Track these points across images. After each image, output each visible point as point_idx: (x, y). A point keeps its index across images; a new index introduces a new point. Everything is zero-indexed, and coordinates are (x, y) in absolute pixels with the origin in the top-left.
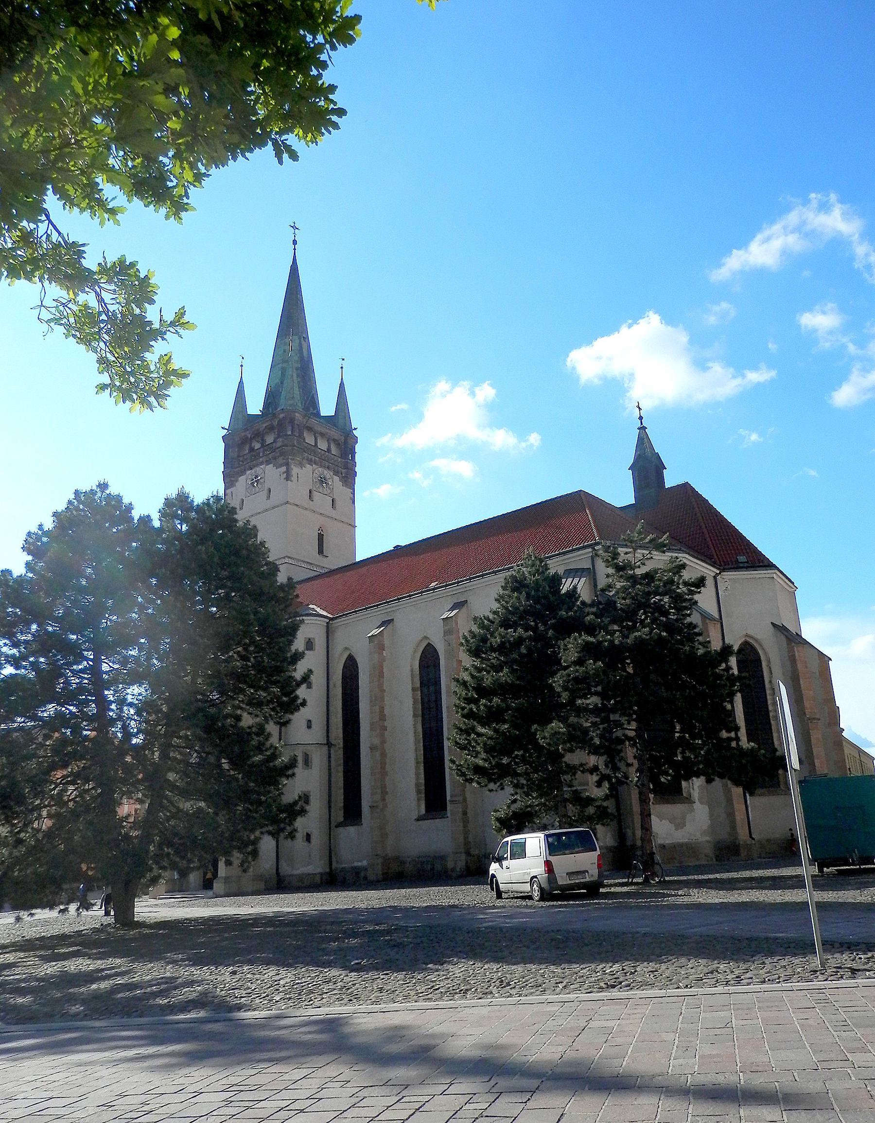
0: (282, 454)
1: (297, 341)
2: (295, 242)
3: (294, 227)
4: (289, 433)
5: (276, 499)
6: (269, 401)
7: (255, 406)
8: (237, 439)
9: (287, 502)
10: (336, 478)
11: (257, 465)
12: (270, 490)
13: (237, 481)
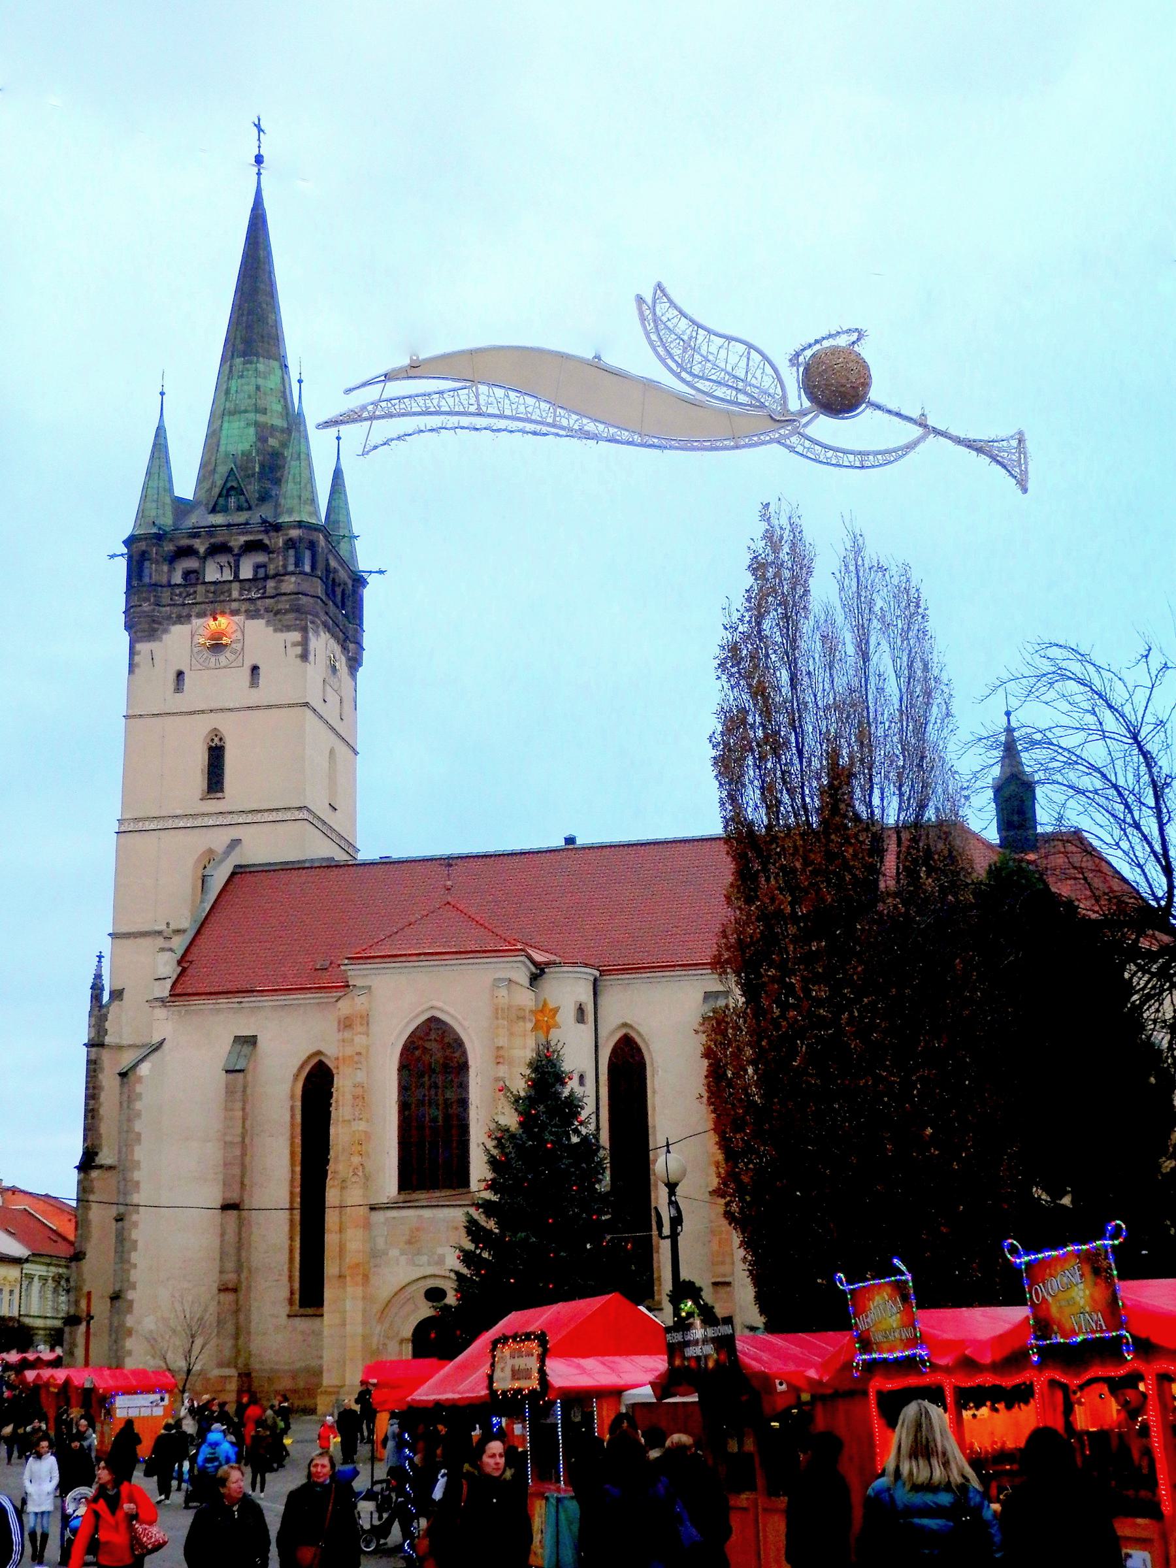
0: (297, 610)
1: (278, 372)
2: (259, 160)
3: (260, 130)
4: (307, 569)
5: (269, 690)
6: (234, 484)
7: (185, 485)
8: (169, 547)
9: (306, 704)
10: (343, 659)
11: (223, 613)
12: (255, 669)
13: (166, 631)
